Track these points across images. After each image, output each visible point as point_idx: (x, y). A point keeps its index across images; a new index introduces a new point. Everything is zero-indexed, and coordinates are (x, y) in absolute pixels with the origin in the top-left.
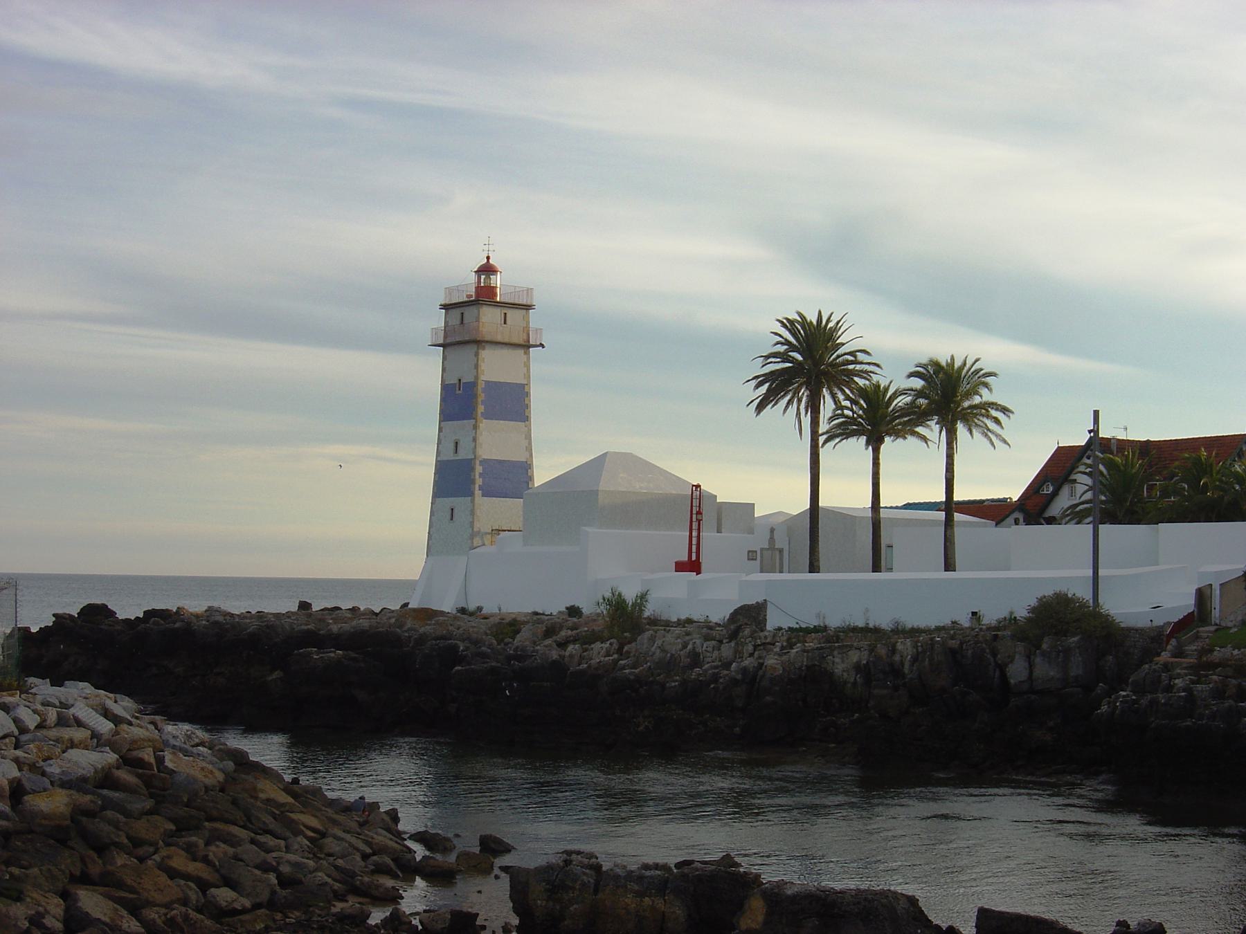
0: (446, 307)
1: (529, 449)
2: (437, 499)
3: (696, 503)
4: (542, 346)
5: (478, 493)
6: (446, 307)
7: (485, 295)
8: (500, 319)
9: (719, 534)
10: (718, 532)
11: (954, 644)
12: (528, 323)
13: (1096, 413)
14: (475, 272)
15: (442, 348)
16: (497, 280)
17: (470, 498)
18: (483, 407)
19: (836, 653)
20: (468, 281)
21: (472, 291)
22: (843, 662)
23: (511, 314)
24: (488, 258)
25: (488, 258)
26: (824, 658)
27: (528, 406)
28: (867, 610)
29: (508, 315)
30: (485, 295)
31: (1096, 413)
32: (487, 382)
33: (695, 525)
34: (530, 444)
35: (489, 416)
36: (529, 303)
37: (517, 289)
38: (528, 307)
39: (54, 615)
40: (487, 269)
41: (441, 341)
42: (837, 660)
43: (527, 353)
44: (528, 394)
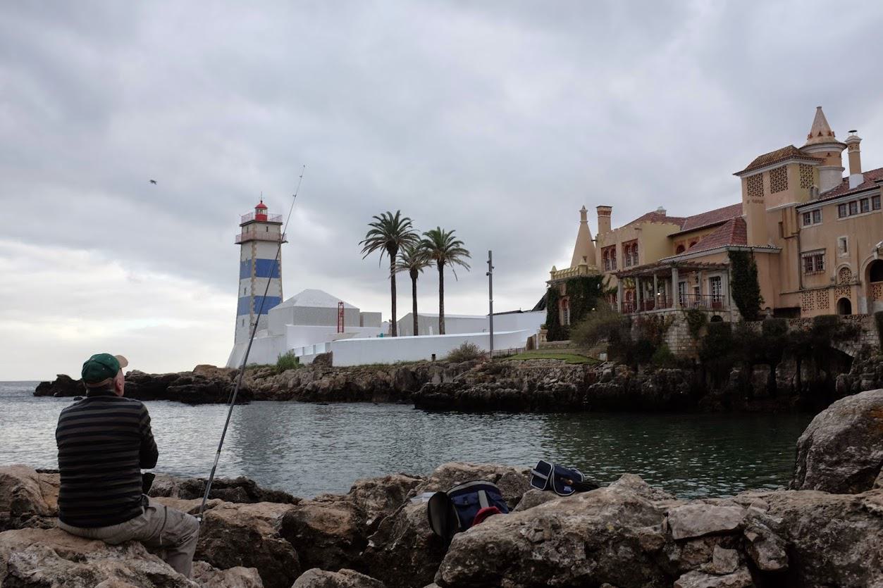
0: (242, 225)
1: (281, 291)
6: (242, 225)
7: (261, 219)
8: (265, 229)
9: (416, 337)
11: (413, 369)
13: (490, 252)
16: (264, 212)
20: (251, 213)
21: (254, 218)
27: (280, 271)
30: (261, 219)
31: (490, 252)
32: (258, 260)
33: (341, 322)
37: (274, 216)
38: (281, 224)
39: (58, 375)
40: (261, 207)
41: (240, 240)
44: (279, 265)
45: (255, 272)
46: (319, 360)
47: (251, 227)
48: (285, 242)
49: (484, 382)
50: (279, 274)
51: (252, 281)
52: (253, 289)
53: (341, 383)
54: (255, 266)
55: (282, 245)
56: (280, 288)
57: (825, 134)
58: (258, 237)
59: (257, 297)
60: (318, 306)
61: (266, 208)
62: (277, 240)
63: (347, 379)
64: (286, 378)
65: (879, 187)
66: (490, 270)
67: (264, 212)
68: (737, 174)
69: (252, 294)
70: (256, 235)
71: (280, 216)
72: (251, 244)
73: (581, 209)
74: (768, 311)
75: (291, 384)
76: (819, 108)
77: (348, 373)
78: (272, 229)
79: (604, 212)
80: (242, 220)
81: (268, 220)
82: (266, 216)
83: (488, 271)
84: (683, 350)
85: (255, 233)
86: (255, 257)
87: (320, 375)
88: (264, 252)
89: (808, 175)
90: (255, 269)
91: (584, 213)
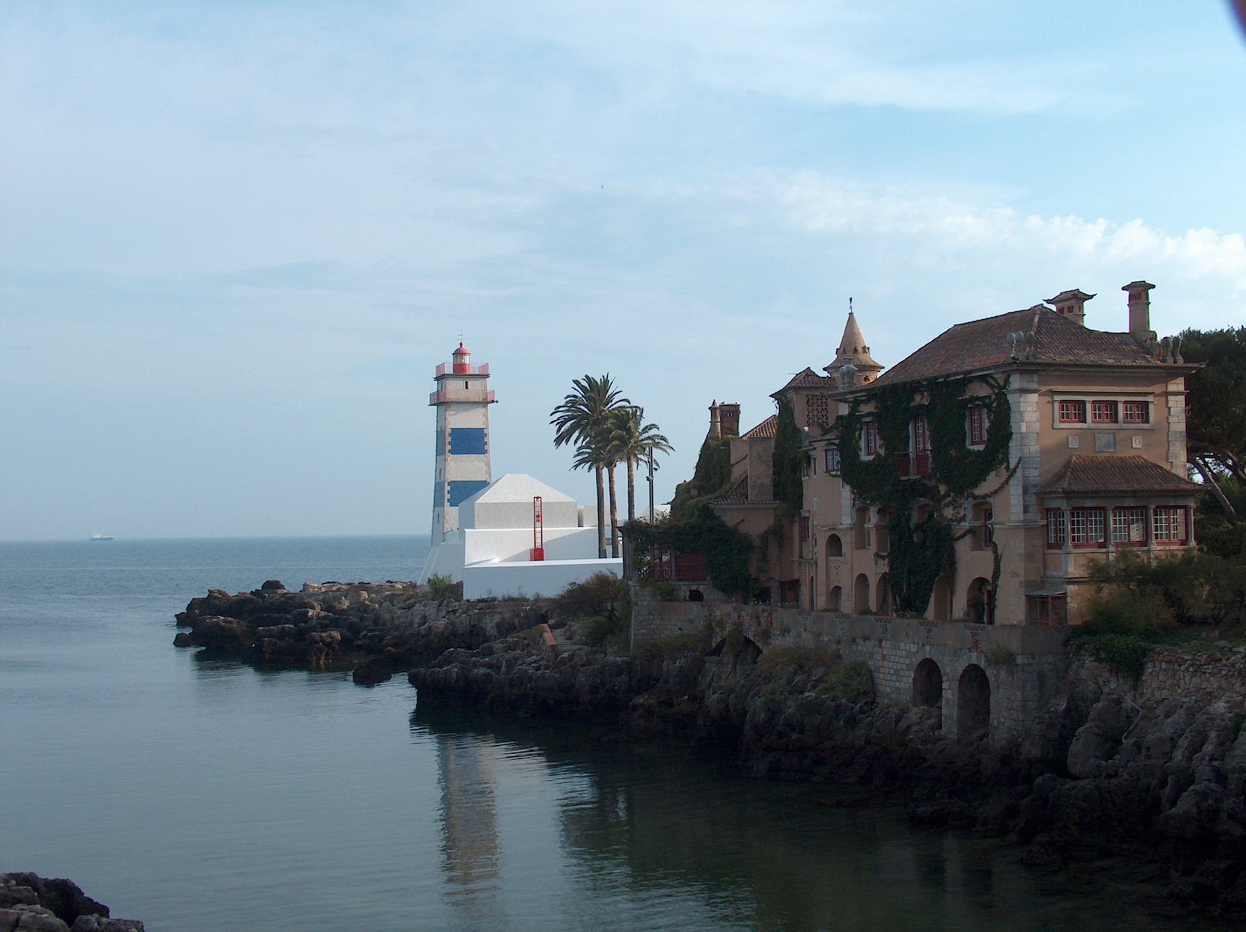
0: (436, 379)
3: (538, 509)
4: (497, 402)
5: (447, 504)
6: (436, 379)
7: (460, 370)
10: (579, 526)
14: (453, 354)
15: (436, 407)
16: (467, 360)
18: (450, 446)
19: (487, 616)
22: (491, 622)
24: (461, 344)
25: (461, 344)
26: (481, 620)
27: (486, 443)
28: (520, 587)
29: (469, 383)
30: (460, 370)
36: (485, 374)
38: (487, 376)
39: (209, 590)
40: (459, 353)
42: (488, 621)
48: (493, 401)
49: (515, 650)
50: (486, 447)
55: (489, 405)
64: (412, 615)
66: (651, 473)
67: (467, 360)
73: (711, 405)
75: (417, 620)
80: (437, 373)
83: (648, 475)
84: (643, 634)
89: (820, 408)
90: (450, 443)
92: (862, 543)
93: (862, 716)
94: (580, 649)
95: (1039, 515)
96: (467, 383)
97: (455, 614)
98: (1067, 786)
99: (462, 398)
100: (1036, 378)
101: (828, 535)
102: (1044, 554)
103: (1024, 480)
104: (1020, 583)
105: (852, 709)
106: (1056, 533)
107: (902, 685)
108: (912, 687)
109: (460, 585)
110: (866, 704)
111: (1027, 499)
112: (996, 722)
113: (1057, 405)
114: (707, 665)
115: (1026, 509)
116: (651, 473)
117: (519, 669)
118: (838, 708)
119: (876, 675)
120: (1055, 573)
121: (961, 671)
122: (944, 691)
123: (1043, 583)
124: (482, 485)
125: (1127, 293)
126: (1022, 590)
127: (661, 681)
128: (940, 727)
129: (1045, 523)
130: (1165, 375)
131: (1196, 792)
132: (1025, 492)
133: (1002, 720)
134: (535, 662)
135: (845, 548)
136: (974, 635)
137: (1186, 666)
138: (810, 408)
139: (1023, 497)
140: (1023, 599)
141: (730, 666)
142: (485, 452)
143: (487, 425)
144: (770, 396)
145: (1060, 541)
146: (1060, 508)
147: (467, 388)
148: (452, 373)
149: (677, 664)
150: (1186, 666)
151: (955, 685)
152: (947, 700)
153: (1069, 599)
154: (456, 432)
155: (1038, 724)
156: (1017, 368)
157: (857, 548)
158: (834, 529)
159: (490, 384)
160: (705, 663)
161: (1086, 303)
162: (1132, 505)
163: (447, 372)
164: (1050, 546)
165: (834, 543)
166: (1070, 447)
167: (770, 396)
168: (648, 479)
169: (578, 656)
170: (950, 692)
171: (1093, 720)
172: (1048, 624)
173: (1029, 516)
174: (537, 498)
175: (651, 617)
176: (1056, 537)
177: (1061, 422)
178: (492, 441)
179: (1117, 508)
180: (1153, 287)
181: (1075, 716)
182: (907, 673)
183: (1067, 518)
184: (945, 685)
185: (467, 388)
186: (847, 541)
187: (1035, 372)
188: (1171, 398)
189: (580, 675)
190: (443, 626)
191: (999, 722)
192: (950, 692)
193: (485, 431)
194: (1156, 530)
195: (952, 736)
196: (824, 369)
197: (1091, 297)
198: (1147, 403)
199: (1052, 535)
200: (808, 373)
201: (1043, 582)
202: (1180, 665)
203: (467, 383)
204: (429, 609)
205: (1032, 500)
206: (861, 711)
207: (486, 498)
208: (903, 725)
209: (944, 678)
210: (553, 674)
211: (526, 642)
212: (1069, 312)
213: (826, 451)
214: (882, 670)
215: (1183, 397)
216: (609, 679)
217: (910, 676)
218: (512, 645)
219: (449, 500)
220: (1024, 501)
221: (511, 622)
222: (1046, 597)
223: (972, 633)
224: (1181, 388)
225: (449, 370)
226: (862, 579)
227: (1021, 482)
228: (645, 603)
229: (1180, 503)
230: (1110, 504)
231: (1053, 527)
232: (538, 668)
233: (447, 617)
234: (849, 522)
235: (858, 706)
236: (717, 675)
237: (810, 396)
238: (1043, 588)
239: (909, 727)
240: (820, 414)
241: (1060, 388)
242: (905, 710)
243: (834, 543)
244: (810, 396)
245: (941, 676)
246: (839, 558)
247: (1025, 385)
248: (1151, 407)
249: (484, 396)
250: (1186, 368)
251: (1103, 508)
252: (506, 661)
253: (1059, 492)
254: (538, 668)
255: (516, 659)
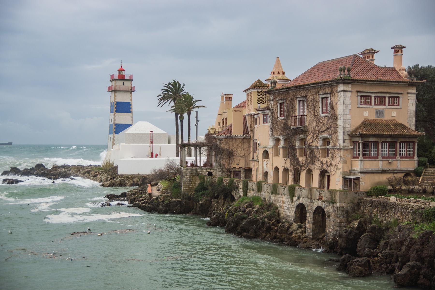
1: (132, 120)
2: (110, 135)
4: (136, 91)
7: (121, 77)
12: (132, 84)
16: (123, 73)
17: (112, 135)
23: (126, 83)
24: (121, 67)
25: (121, 67)
27: (131, 108)
32: (117, 102)
34: (133, 119)
35: (116, 111)
38: (132, 80)
40: (121, 70)
43: (131, 93)
44: (131, 105)
45: (116, 110)
46: (110, 170)
47: (114, 82)
48: (134, 91)
49: (136, 195)
51: (114, 115)
52: (115, 120)
53: (118, 184)
54: (116, 106)
56: (131, 119)
57: (281, 73)
58: (118, 89)
59: (116, 124)
60: (141, 132)
61: (124, 71)
62: (129, 90)
63: (120, 182)
65: (259, 114)
66: (197, 123)
68: (245, 91)
69: (114, 123)
70: (116, 88)
71: (131, 76)
72: (113, 93)
74: (241, 169)
76: (278, 57)
77: (123, 178)
78: (127, 84)
79: (228, 98)
81: (126, 78)
82: (124, 75)
84: (186, 189)
85: (116, 86)
86: (116, 101)
87: (109, 179)
88: (123, 98)
89: (263, 97)
90: (116, 108)
91: (222, 97)
92: (277, 154)
93: (273, 226)
94: (161, 195)
95: (350, 144)
96: (123, 83)
97: (114, 179)
98: (355, 260)
99: (121, 90)
100: (350, 86)
101: (264, 150)
102: (351, 160)
103: (343, 129)
104: (341, 172)
105: (269, 223)
106: (356, 152)
107: (290, 214)
108: (294, 215)
109: (116, 167)
110: (275, 221)
111: (344, 137)
112: (328, 231)
113: (359, 97)
114: (213, 203)
115: (344, 142)
116: (197, 123)
117: (135, 203)
118: (264, 223)
119: (279, 209)
120: (355, 169)
121: (314, 209)
122: (307, 217)
123: (351, 172)
124: (128, 126)
125: (393, 50)
126: (341, 175)
127: (194, 209)
128: (305, 232)
129: (352, 148)
130: (407, 86)
131: (410, 265)
132: (344, 134)
133: (331, 230)
134: (143, 200)
135: (270, 155)
136: (320, 194)
137: (409, 210)
138: (259, 97)
139: (343, 136)
140: (342, 178)
141: (222, 204)
142: (130, 112)
143: (132, 101)
144: (243, 91)
145: (358, 155)
146: (358, 141)
147: (123, 85)
148: (117, 78)
149: (200, 202)
150: (409, 210)
151: (312, 214)
152: (308, 221)
153: (361, 180)
154: (118, 104)
155: (345, 232)
156: (342, 81)
157: (275, 156)
158: (266, 147)
159: (134, 84)
160: (212, 202)
161: (375, 54)
162: (390, 141)
163: (115, 78)
164: (354, 157)
165: (266, 154)
166: (364, 115)
167: (243, 91)
168: (196, 125)
169: (160, 198)
170: (309, 217)
171: (368, 232)
172: (351, 190)
173: (345, 144)
174: (151, 132)
175: (191, 183)
176: (356, 154)
177: (360, 105)
178: (134, 108)
179: (383, 142)
180: (405, 47)
181: (361, 229)
182: (292, 209)
183: (361, 146)
184: (308, 215)
185: (123, 85)
186: (271, 153)
187: (350, 83)
188: (409, 95)
189: (160, 206)
190: (108, 184)
191: (329, 231)
192: (310, 217)
193: (131, 103)
194: (400, 151)
195: (310, 236)
196: (266, 81)
197: (378, 52)
198: (399, 97)
199: (355, 153)
200: (259, 81)
201: (350, 172)
202: (406, 210)
203: (123, 83)
204: (103, 177)
205: (347, 137)
206: (273, 224)
207: (129, 131)
208: (291, 230)
209: (308, 212)
210: (149, 205)
211: (141, 191)
212: (368, 58)
213: (263, 115)
214: (282, 207)
215: (415, 95)
216: (172, 208)
217: (294, 210)
218: (134, 193)
219: (115, 132)
220: (343, 138)
221: (137, 183)
222: (351, 179)
223: (319, 193)
224: (414, 91)
225: (116, 77)
226: (277, 169)
227: (342, 130)
228: (188, 177)
229: (411, 140)
230: (380, 140)
231: (355, 149)
232: (144, 203)
233: (110, 181)
234: (272, 145)
235: (272, 222)
236: (216, 207)
237: (259, 92)
238: (351, 175)
239: (292, 232)
240: (263, 99)
241: (361, 90)
242: (291, 225)
243: (266, 154)
244: (259, 92)
245: (306, 211)
246: (267, 160)
247: (345, 89)
248: (401, 99)
249: (131, 88)
250: (417, 82)
251: (378, 142)
252: (130, 199)
253: (358, 135)
254: (144, 203)
255: (135, 199)
